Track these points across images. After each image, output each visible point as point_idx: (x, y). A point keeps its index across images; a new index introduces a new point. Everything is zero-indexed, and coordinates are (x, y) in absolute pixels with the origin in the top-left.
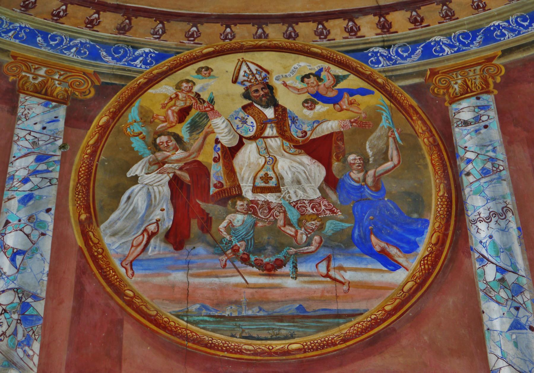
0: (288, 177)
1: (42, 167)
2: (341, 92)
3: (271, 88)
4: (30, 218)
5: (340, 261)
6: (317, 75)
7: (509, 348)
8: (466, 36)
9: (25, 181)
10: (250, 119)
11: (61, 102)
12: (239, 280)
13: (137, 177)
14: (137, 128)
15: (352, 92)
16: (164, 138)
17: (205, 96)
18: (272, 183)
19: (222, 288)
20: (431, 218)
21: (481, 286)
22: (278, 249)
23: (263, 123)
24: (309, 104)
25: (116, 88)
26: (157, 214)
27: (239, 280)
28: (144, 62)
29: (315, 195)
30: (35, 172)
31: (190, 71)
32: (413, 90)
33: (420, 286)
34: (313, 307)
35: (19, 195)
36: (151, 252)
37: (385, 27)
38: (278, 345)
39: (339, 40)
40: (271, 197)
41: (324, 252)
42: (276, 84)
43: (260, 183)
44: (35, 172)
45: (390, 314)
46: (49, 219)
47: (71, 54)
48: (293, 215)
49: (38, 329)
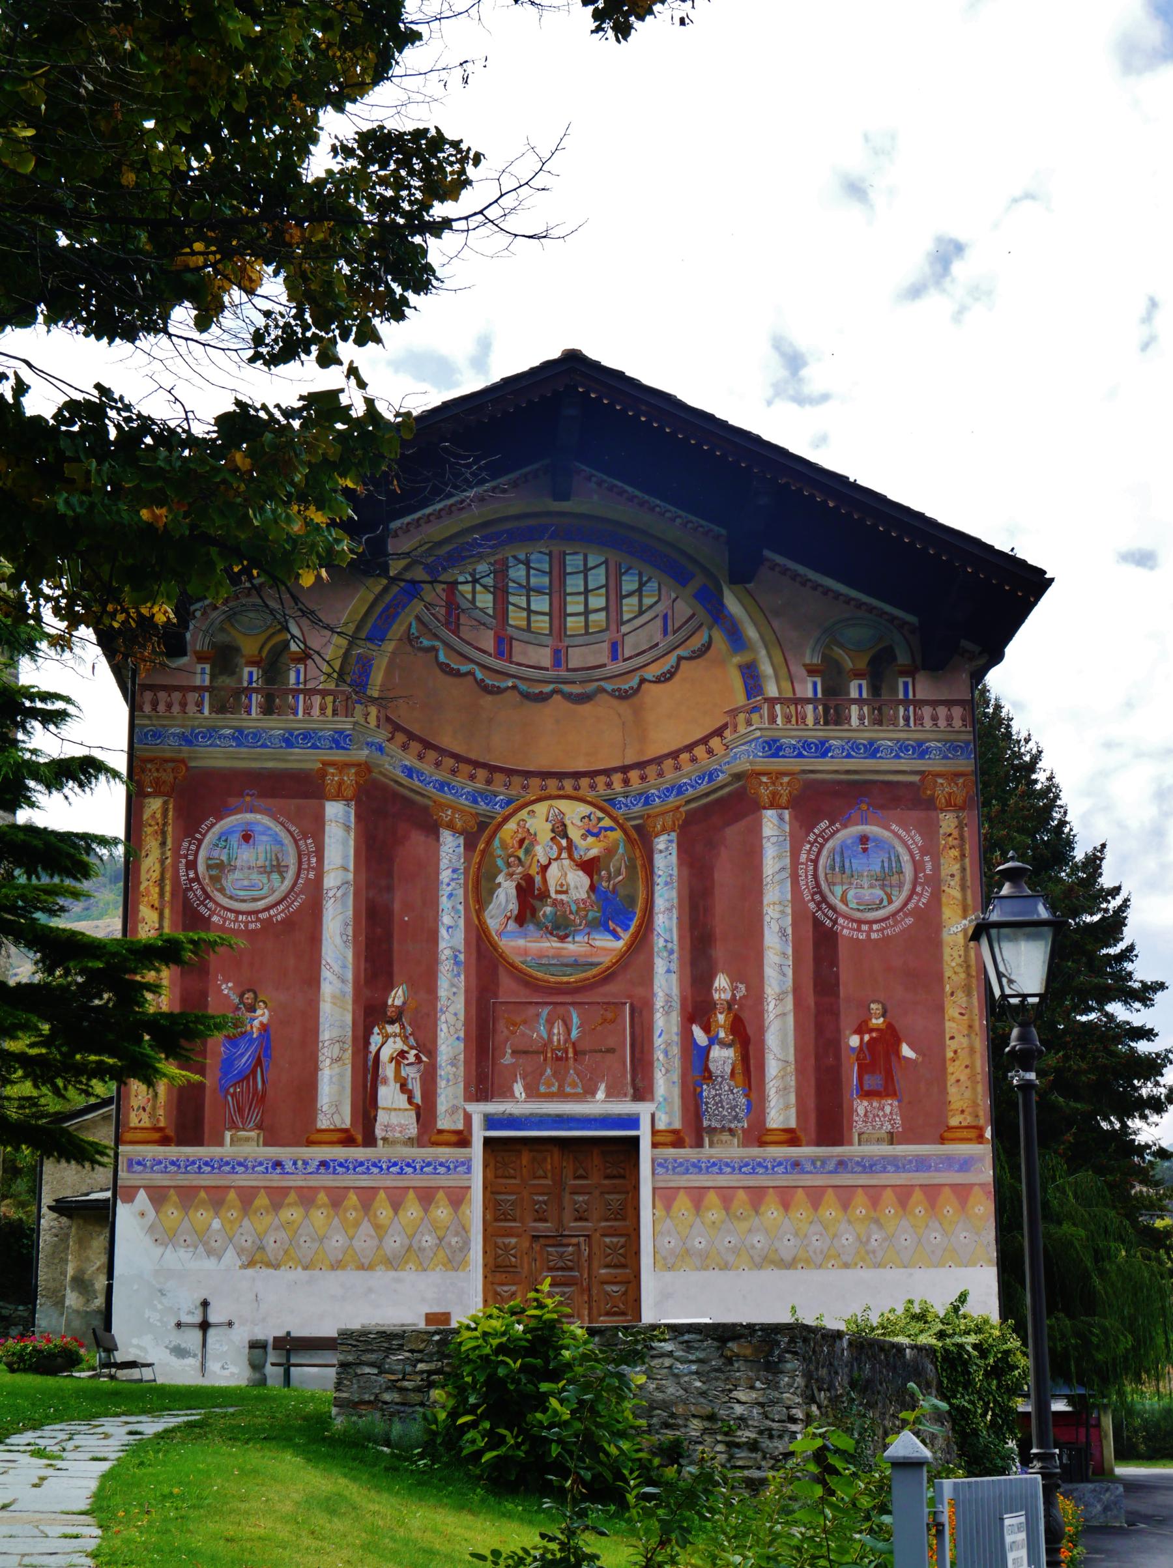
0: (572, 885)
1: (455, 876)
2: (601, 828)
3: (565, 825)
4: (453, 907)
5: (595, 935)
6: (589, 817)
7: (664, 983)
8: (668, 790)
9: (448, 885)
10: (555, 847)
11: (461, 834)
12: (548, 944)
13: (499, 884)
14: (499, 852)
15: (606, 829)
16: (512, 859)
17: (532, 831)
18: (564, 888)
19: (541, 949)
20: (638, 911)
21: (656, 949)
22: (566, 928)
23: (561, 849)
24: (584, 837)
25: (488, 824)
26: (511, 906)
27: (548, 944)
28: (501, 806)
29: (584, 896)
30: (453, 879)
31: (523, 814)
32: (636, 827)
33: (629, 949)
34: (581, 960)
35: (446, 894)
36: (509, 928)
37: (626, 782)
38: (565, 979)
39: (602, 792)
40: (563, 897)
41: (587, 930)
42: (567, 822)
43: (559, 888)
44: (453, 879)
45: (614, 964)
46: (461, 908)
47: (463, 800)
48: (574, 908)
49: (462, 968)
